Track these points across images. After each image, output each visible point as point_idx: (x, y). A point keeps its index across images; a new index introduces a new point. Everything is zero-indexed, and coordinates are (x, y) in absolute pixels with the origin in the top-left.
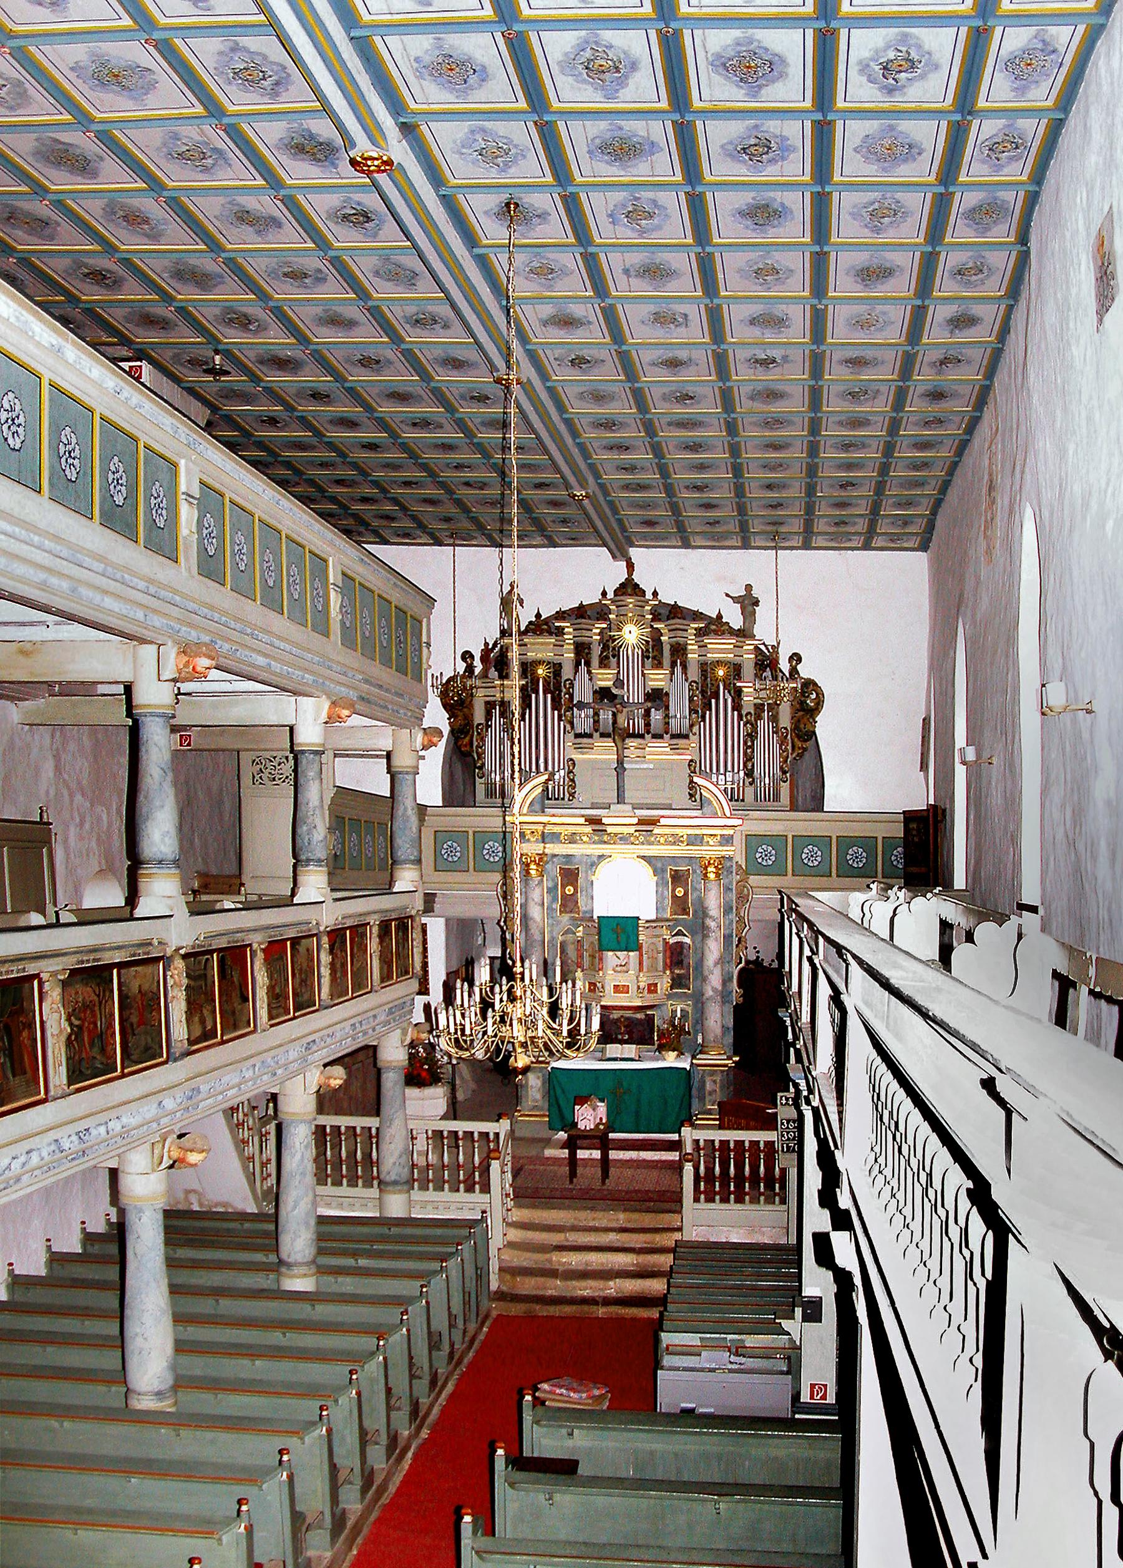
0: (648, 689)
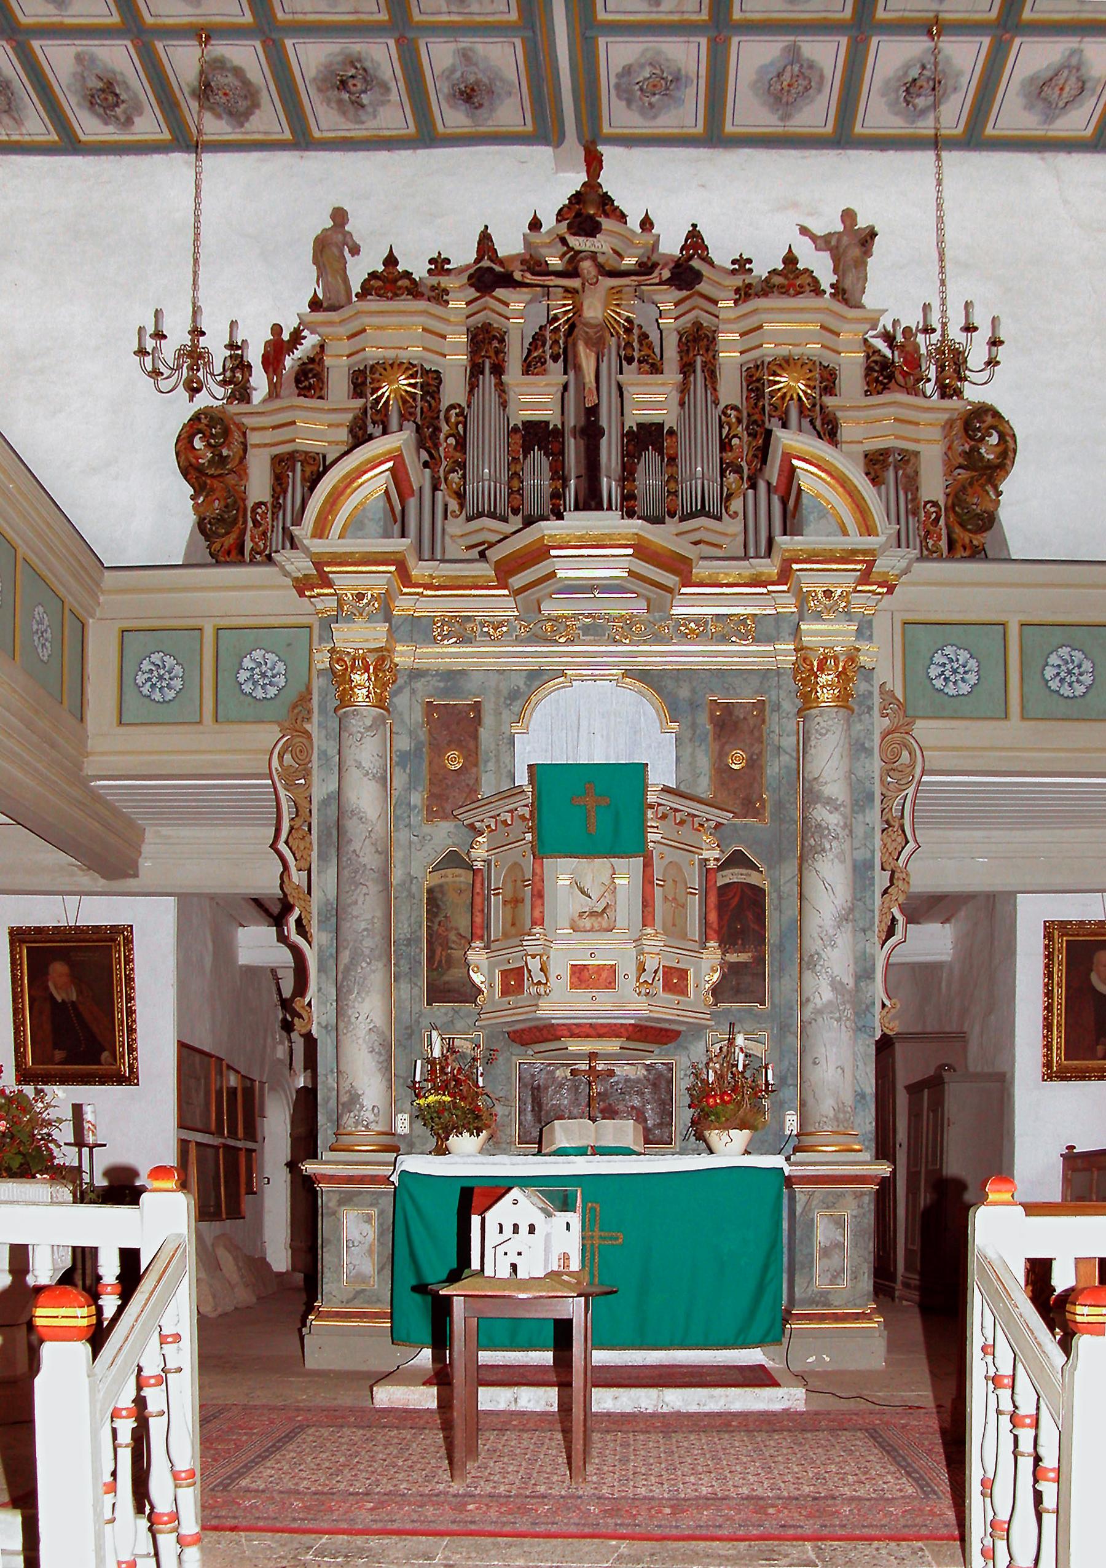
0: (630, 423)
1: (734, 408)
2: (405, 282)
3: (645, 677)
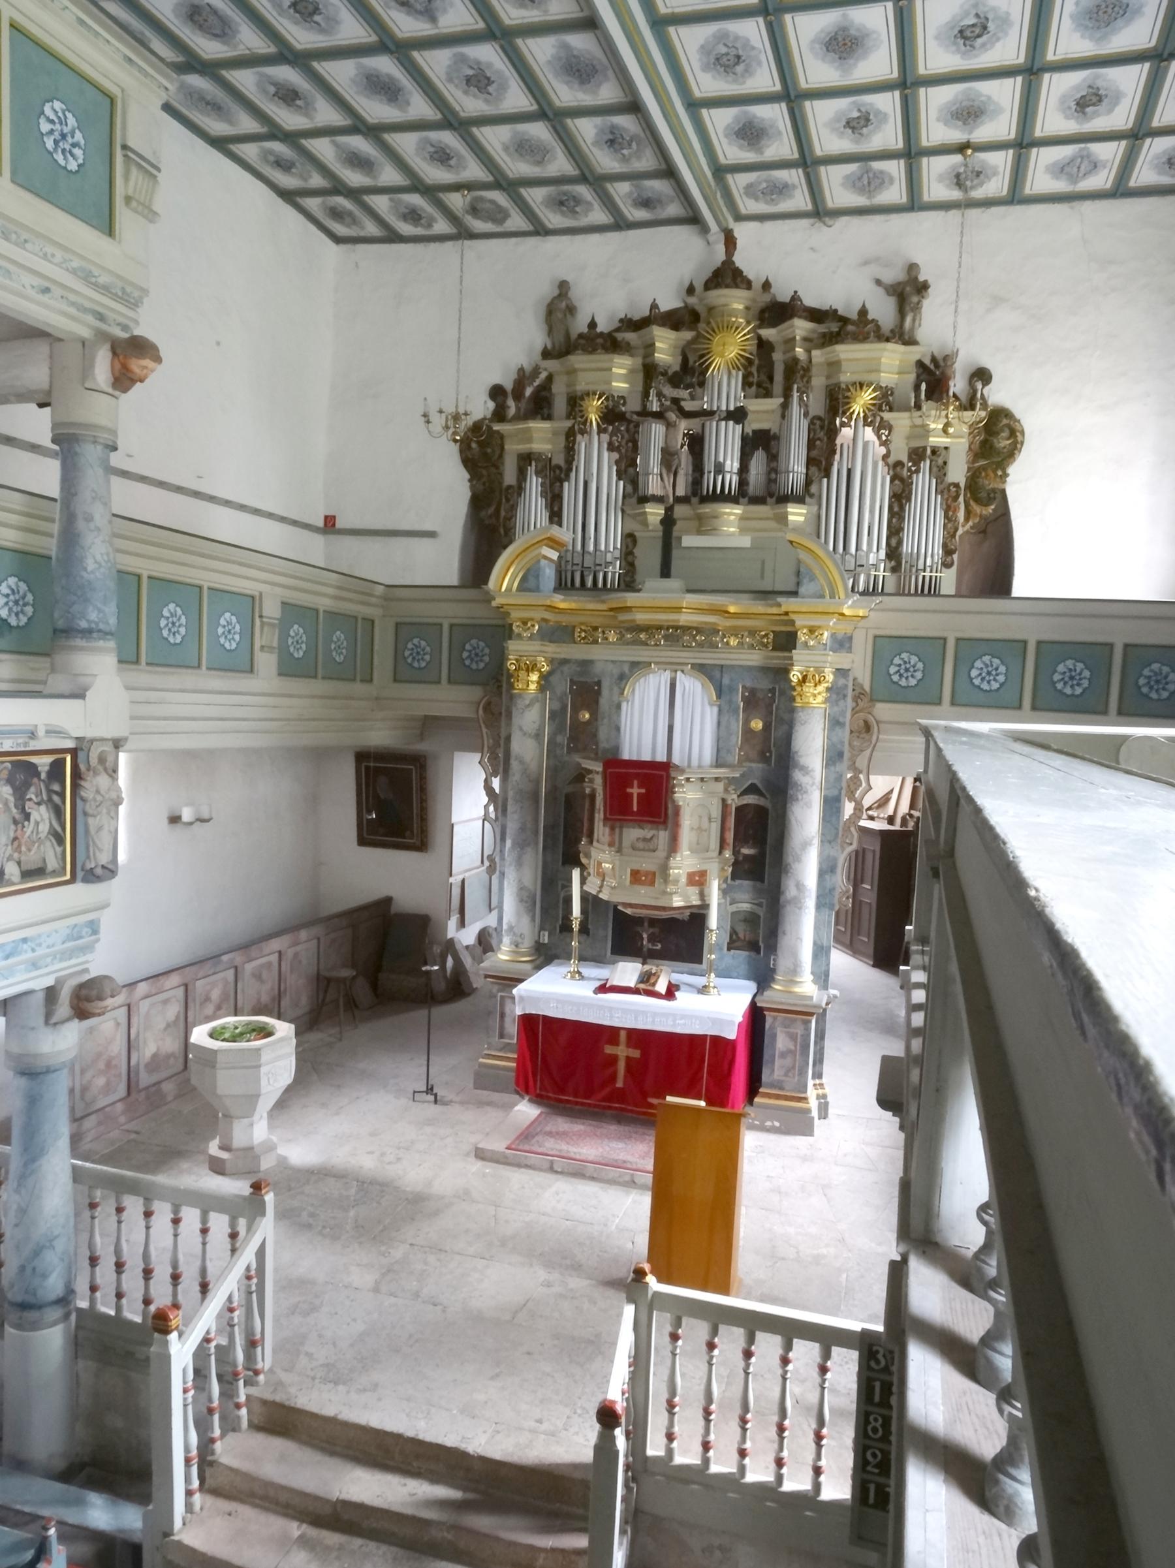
1: (819, 418)
2: (600, 341)
3: (701, 669)
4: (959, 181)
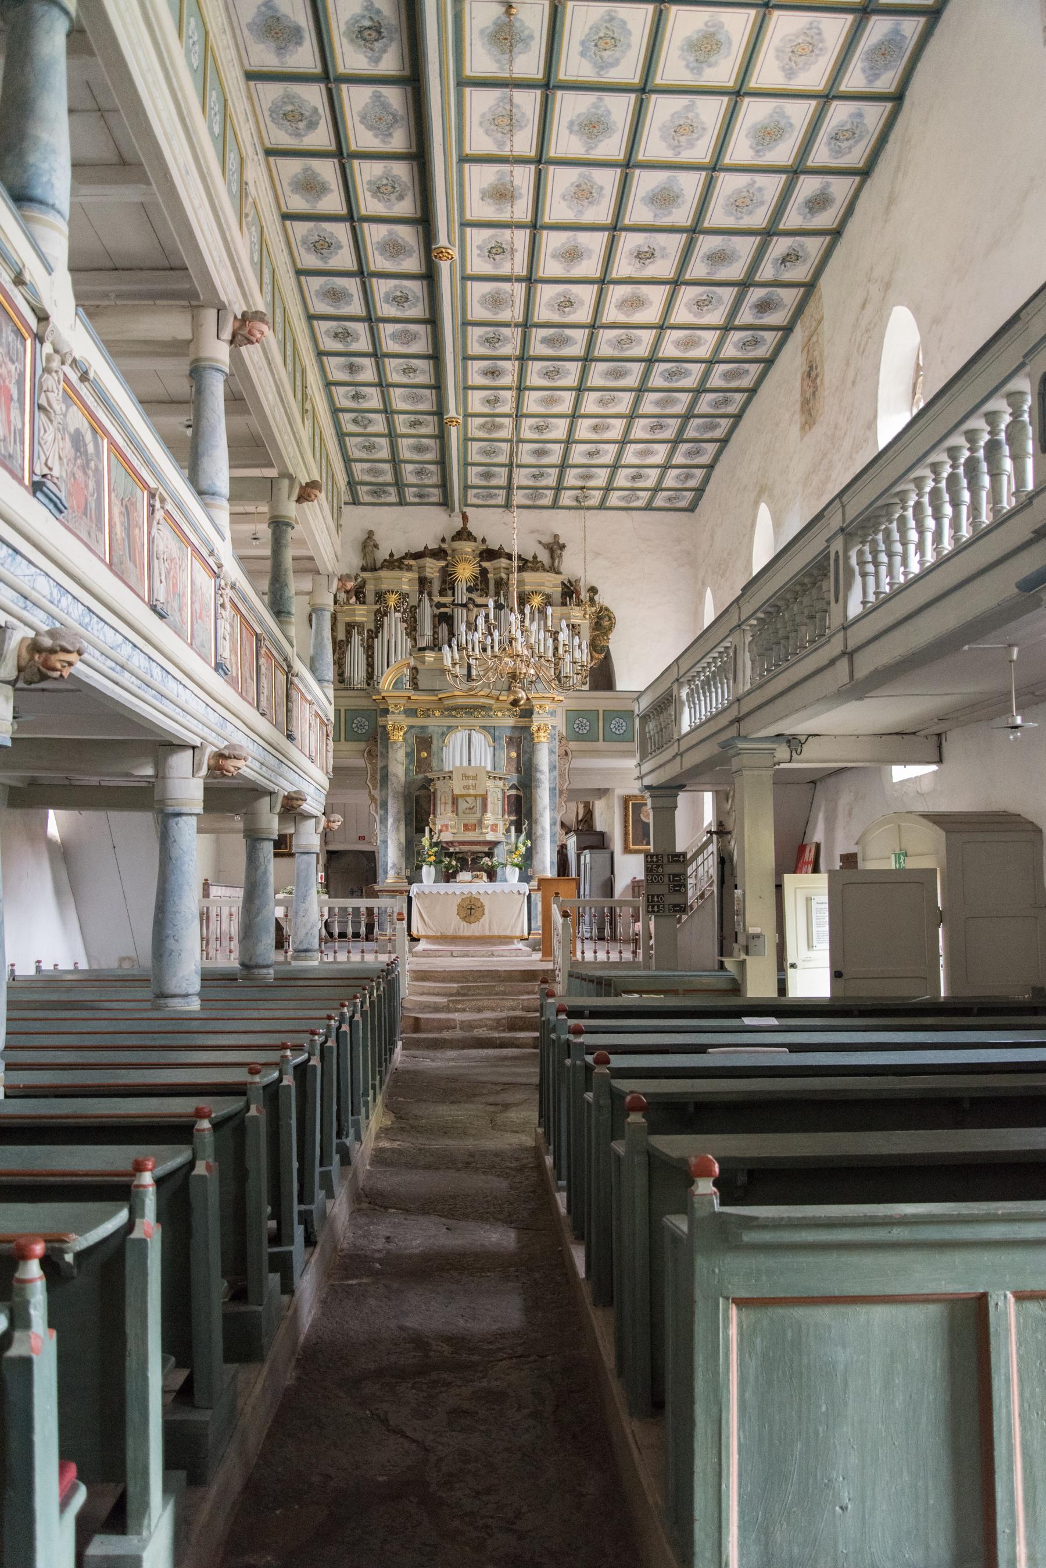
3: (484, 728)
4: (577, 499)
